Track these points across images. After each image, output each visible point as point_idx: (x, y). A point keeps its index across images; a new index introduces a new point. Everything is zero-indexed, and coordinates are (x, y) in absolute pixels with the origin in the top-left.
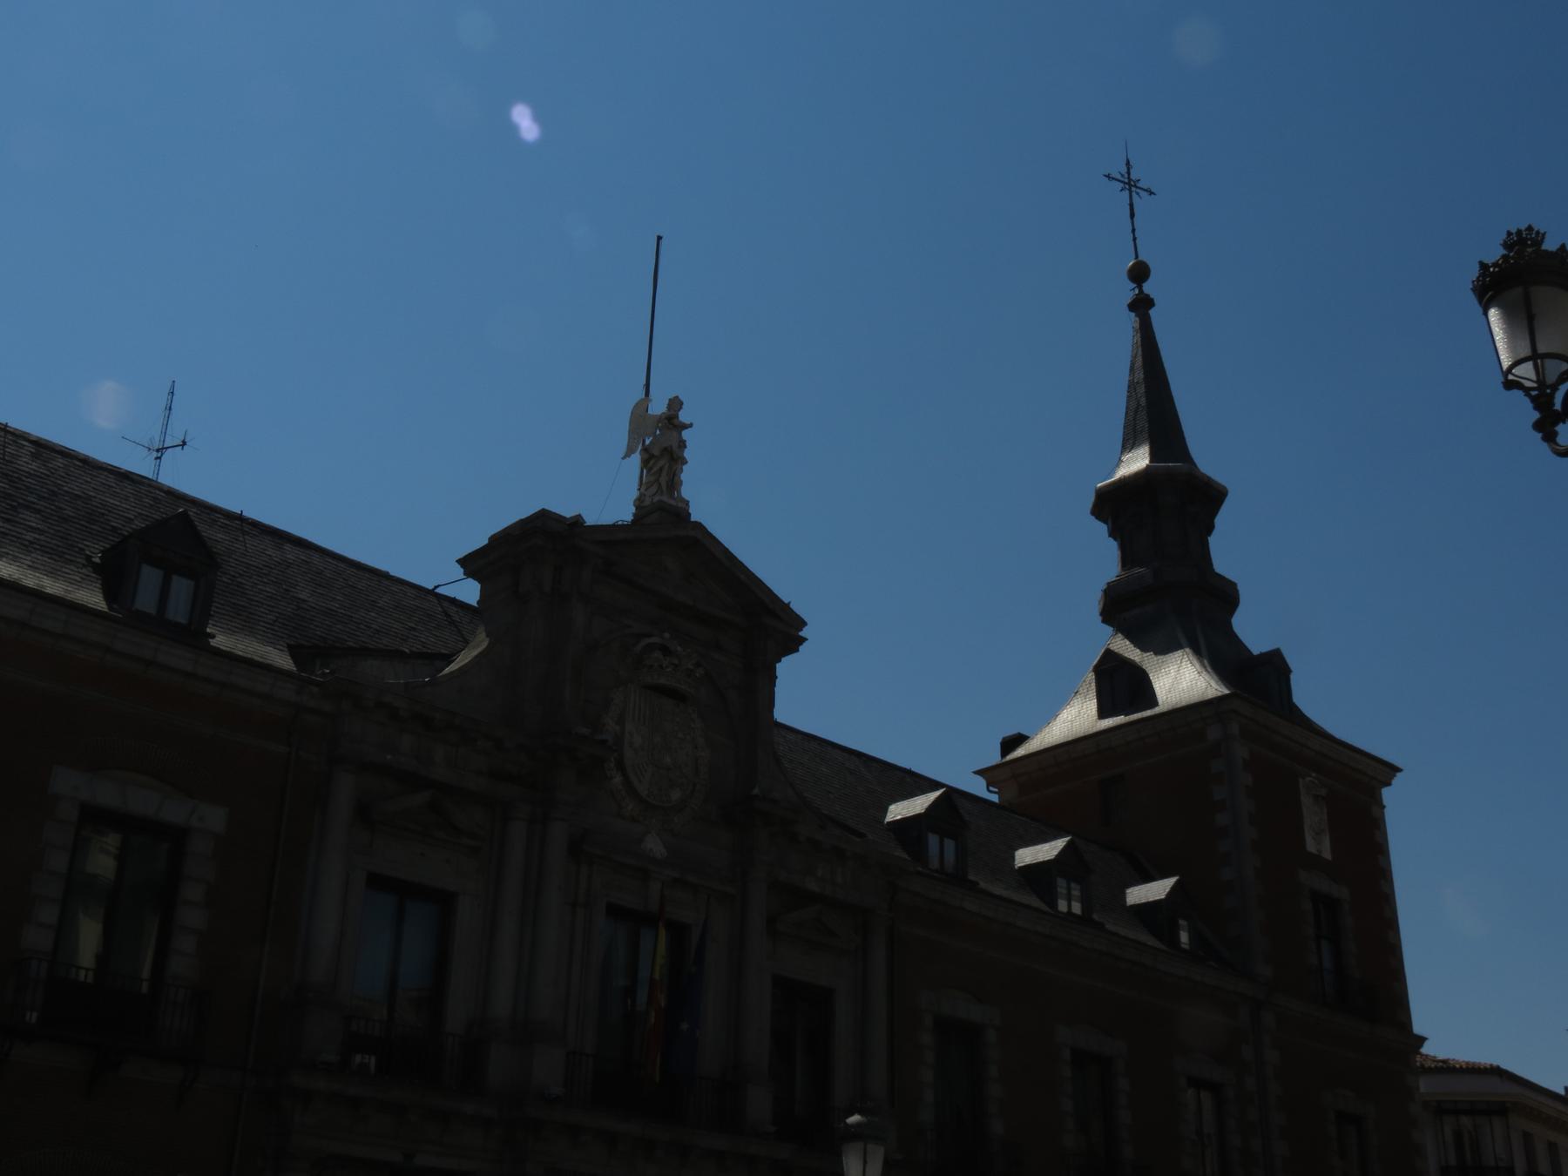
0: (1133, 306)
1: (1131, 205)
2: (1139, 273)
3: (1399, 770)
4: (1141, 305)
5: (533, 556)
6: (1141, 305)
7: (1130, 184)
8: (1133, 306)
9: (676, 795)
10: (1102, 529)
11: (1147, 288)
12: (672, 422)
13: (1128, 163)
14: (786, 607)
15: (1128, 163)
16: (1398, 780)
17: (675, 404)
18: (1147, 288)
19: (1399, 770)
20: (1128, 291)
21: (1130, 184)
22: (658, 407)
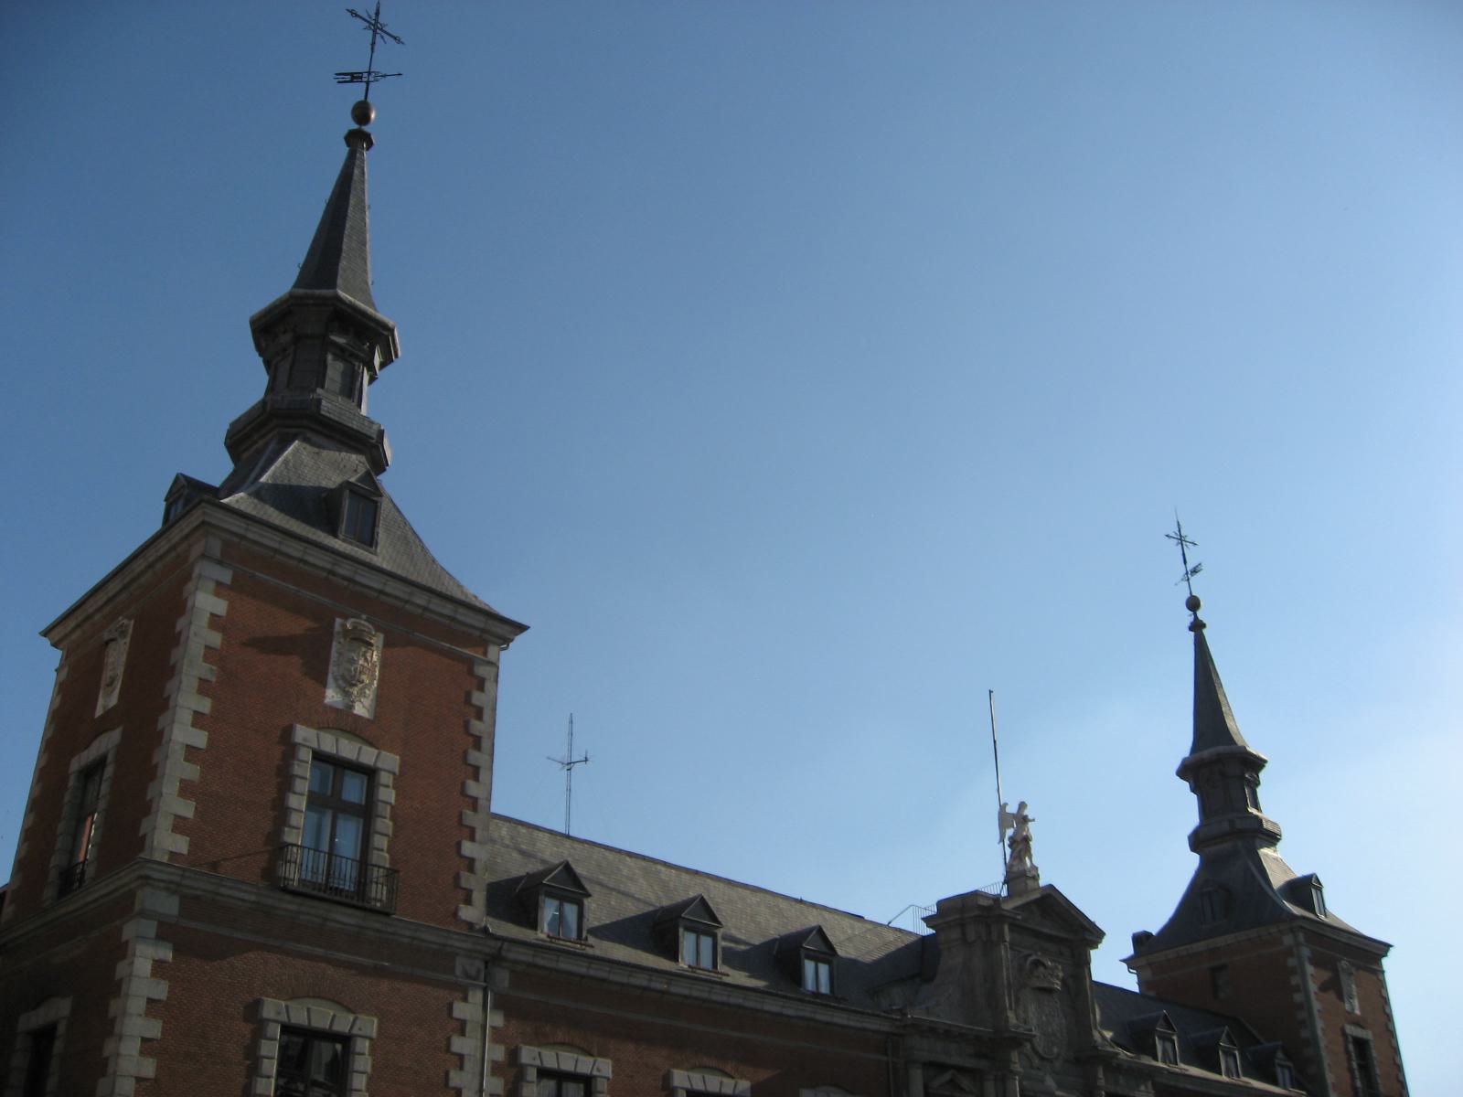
0: (1191, 629)
1: (1184, 555)
2: (1193, 604)
3: (1391, 946)
4: (1197, 626)
5: (961, 915)
6: (1197, 626)
7: (1181, 540)
8: (1191, 629)
9: (1055, 1050)
10: (1186, 785)
11: (1200, 614)
12: (1023, 820)
13: (1179, 525)
14: (1093, 924)
15: (1179, 525)
16: (1392, 952)
17: (1022, 805)
18: (1200, 614)
19: (1391, 946)
20: (1187, 618)
21: (1181, 540)
22: (1012, 809)
